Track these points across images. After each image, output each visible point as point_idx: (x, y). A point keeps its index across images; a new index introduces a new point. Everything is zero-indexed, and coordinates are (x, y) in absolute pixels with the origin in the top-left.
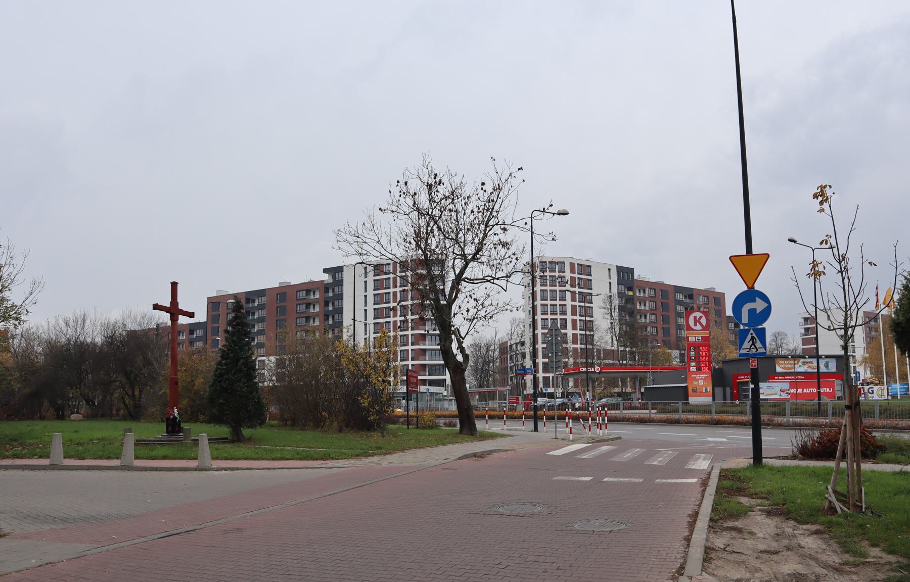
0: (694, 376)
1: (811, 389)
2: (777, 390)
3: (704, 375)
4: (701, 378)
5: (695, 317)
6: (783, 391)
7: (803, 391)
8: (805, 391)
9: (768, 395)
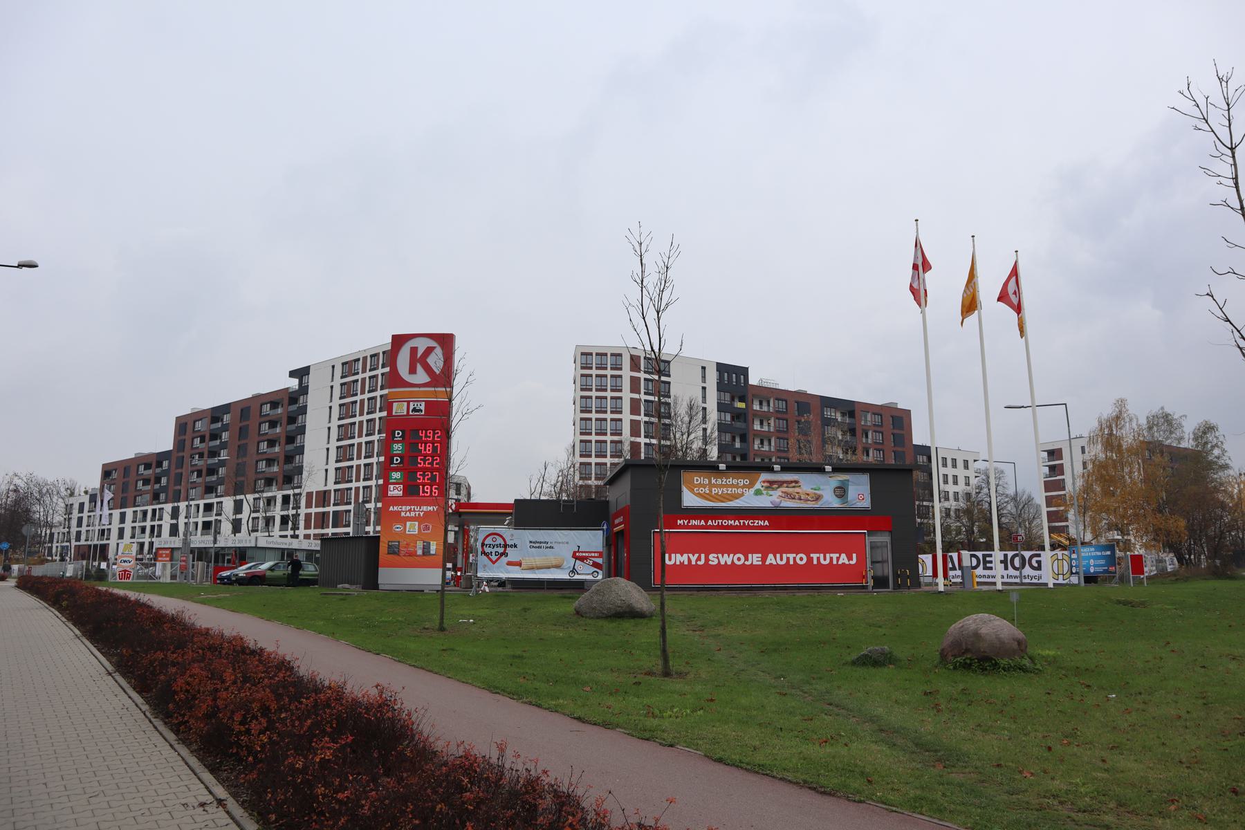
0: (396, 508)
1: (791, 556)
2: (565, 554)
3: (425, 508)
4: (413, 514)
5: (414, 350)
6: (582, 559)
7: (764, 559)
8: (771, 559)
9: (532, 568)
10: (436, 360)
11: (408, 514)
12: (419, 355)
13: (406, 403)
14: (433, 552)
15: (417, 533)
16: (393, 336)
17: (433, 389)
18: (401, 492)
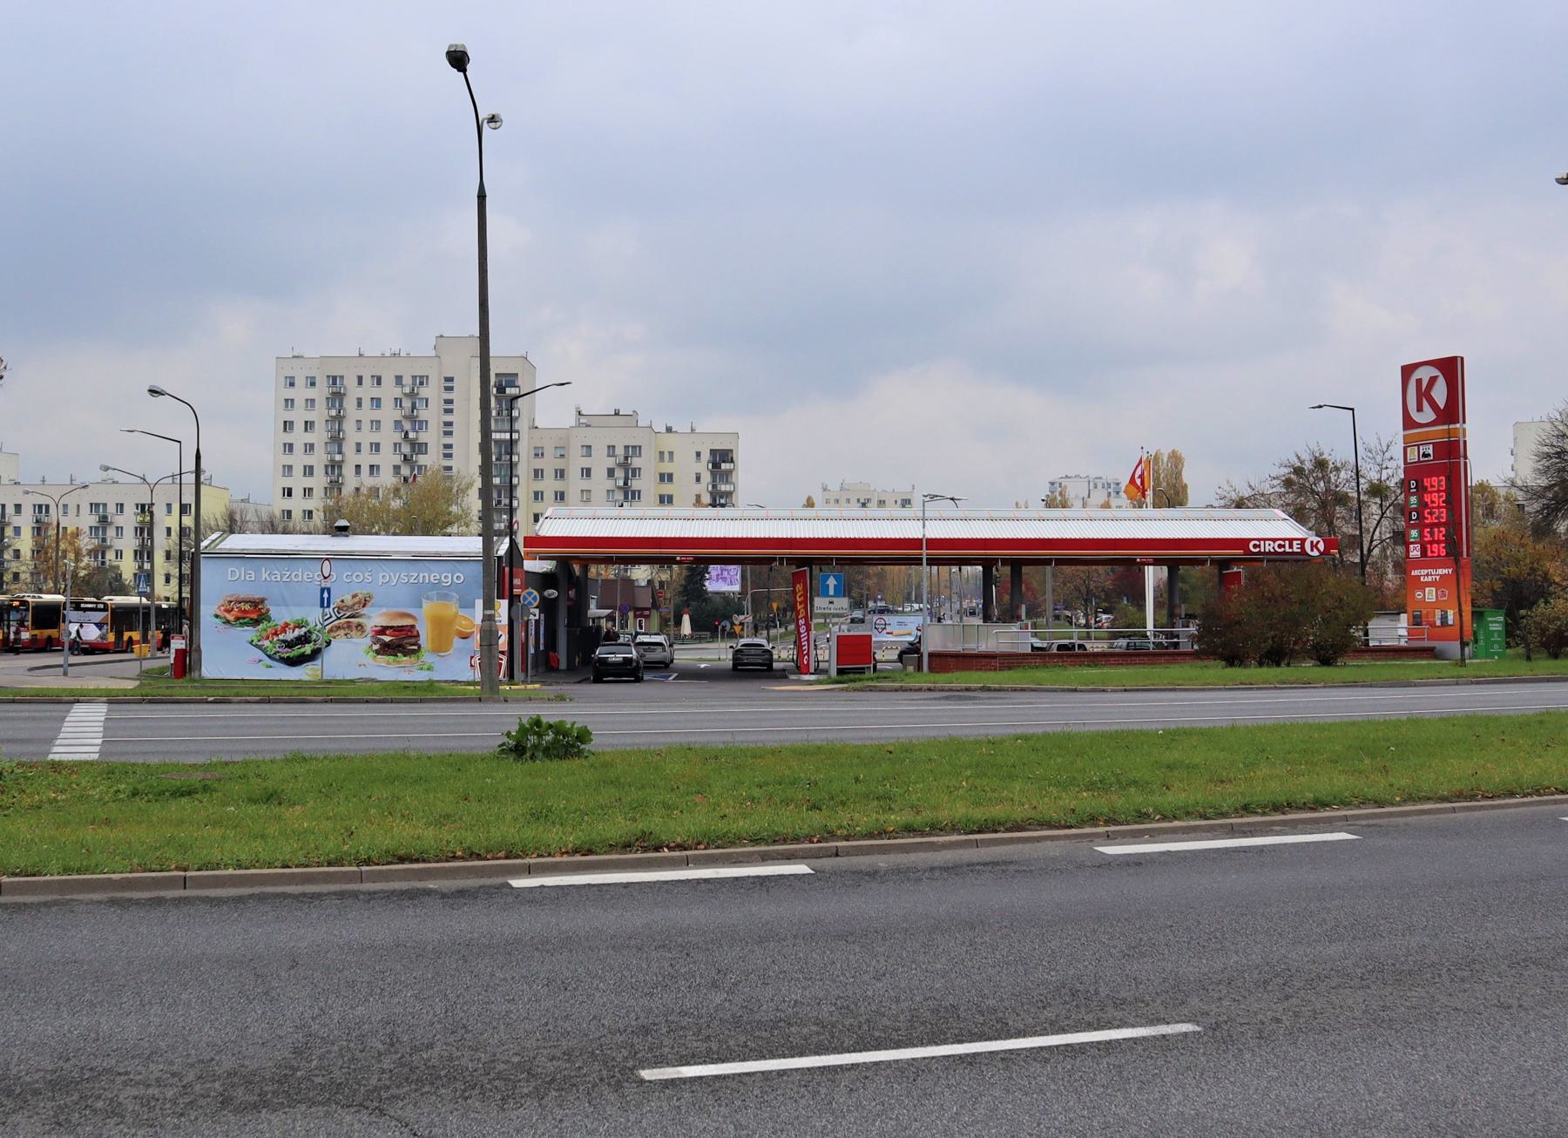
3: (1440, 571)
4: (1430, 579)
10: (1440, 394)
11: (1426, 579)
12: (1423, 389)
13: (1416, 448)
14: (1450, 622)
15: (1434, 600)
16: (1402, 367)
17: (1446, 427)
18: (1419, 553)
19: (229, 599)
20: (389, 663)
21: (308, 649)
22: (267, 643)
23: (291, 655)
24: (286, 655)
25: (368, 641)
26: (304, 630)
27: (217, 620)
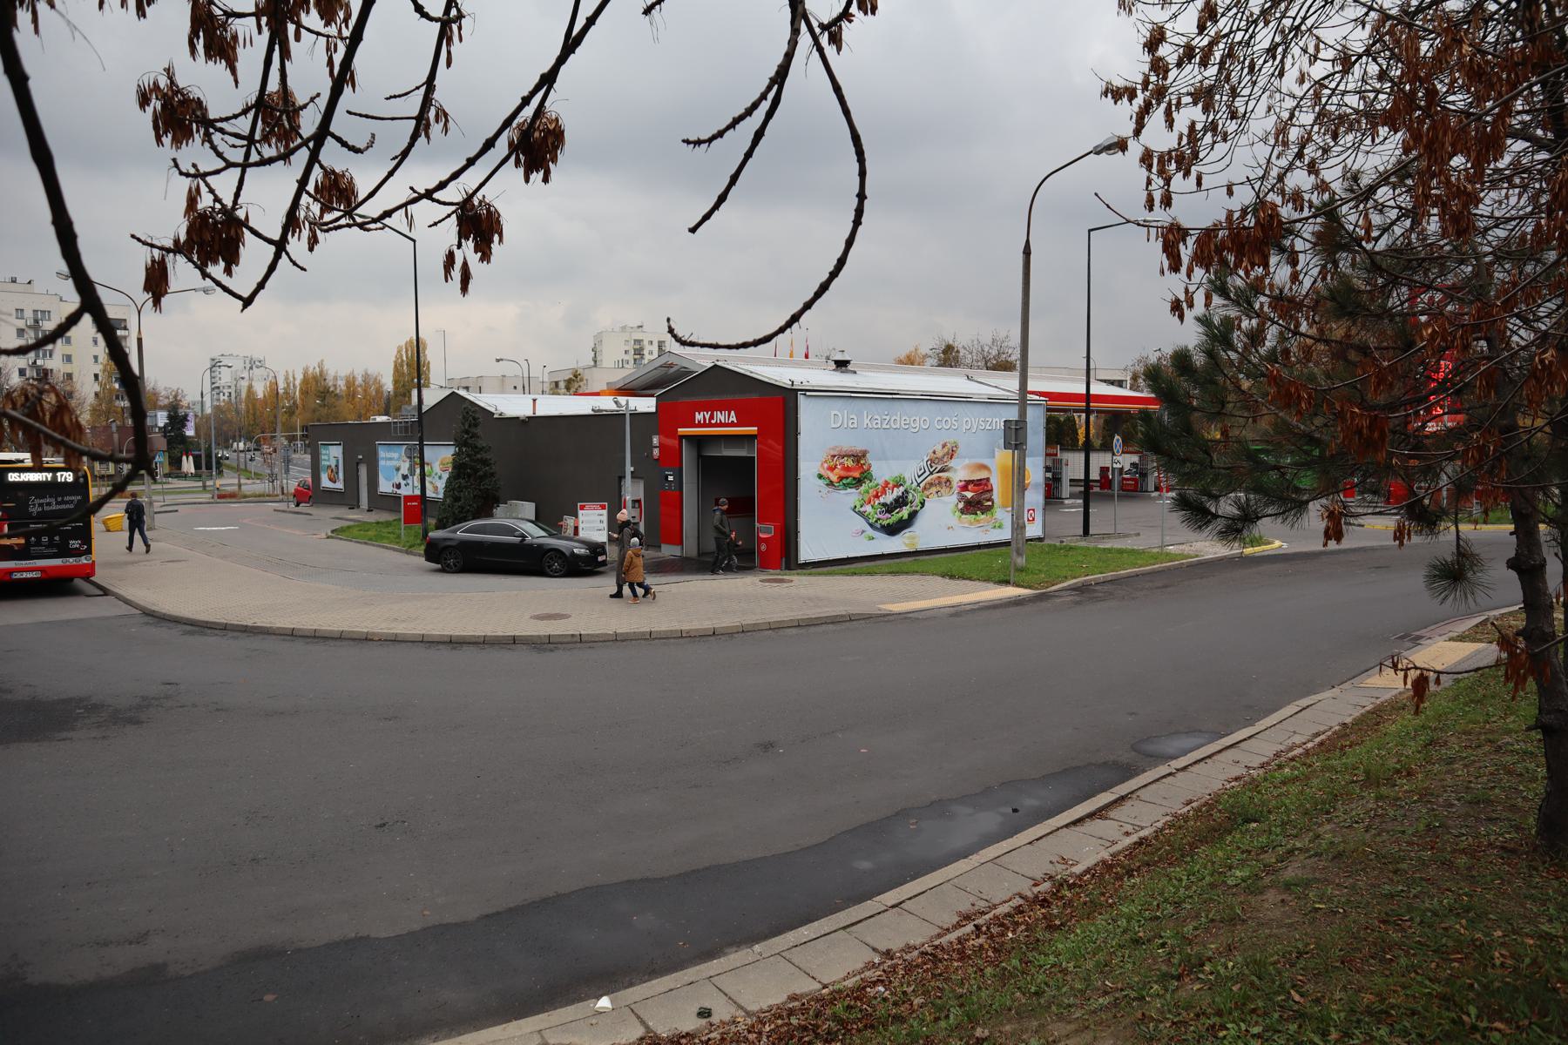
19: (833, 453)
20: (971, 524)
21: (905, 513)
22: (868, 508)
23: (890, 521)
24: (885, 523)
25: (954, 498)
26: (902, 489)
27: (821, 482)
